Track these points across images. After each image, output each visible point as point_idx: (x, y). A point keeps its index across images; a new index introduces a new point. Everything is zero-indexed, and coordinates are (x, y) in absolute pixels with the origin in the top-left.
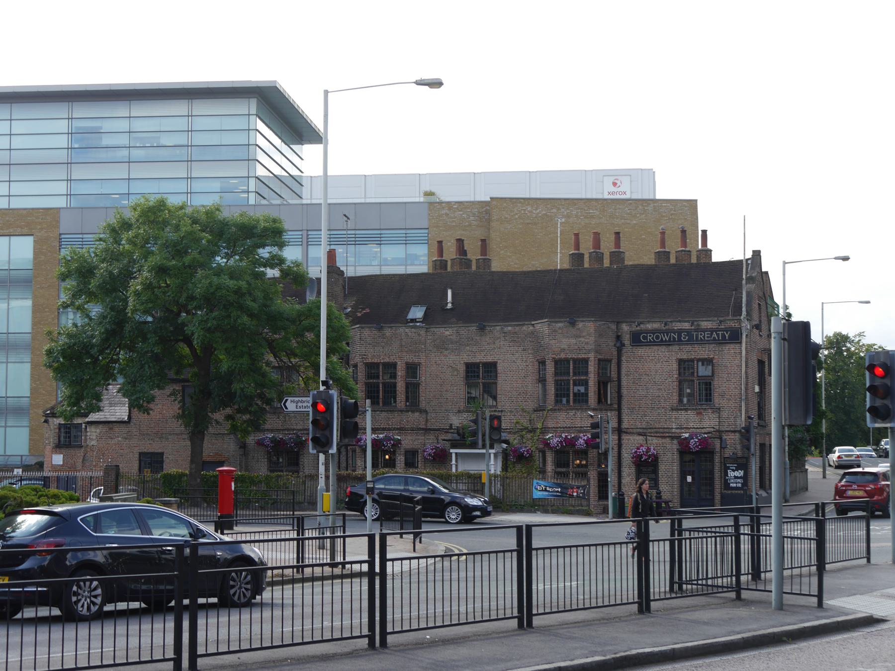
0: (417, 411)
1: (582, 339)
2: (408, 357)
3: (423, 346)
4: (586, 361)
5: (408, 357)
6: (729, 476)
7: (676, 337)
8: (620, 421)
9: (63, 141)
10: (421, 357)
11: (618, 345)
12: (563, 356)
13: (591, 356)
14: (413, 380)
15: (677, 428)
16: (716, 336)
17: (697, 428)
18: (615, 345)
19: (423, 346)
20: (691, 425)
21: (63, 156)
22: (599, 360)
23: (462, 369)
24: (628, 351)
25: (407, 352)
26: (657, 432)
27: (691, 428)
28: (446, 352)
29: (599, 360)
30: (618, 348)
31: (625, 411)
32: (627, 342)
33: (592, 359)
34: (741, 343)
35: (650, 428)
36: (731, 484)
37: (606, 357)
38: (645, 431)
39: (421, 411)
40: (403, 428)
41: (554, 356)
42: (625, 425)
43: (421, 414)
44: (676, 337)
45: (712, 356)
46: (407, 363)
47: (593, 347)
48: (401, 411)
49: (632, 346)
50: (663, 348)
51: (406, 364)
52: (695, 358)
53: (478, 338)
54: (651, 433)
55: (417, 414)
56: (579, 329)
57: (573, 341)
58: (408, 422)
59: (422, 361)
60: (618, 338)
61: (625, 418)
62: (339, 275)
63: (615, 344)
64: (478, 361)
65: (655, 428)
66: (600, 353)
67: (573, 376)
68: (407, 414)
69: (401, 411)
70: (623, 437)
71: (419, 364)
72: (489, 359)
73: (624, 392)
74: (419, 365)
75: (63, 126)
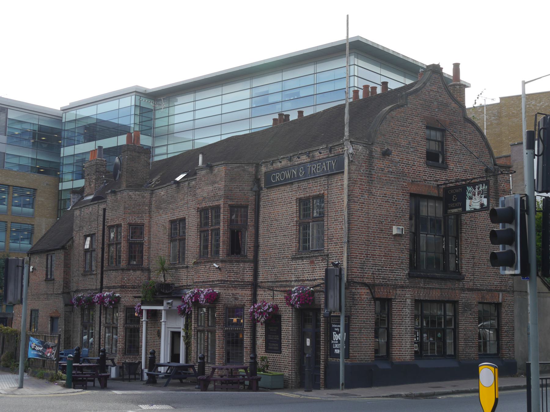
0: (138, 270)
1: (216, 185)
2: (131, 218)
3: (147, 208)
4: (218, 207)
5: (131, 218)
6: (334, 340)
7: (295, 173)
8: (256, 274)
9: (247, 104)
10: (144, 218)
11: (255, 188)
12: (204, 205)
13: (221, 202)
14: (138, 240)
15: (296, 281)
16: (325, 167)
17: (310, 280)
18: (251, 189)
19: (147, 208)
20: (306, 276)
21: (247, 114)
22: (231, 206)
23: (168, 225)
24: (264, 192)
25: (129, 213)
26: (281, 286)
27: (306, 280)
28: (161, 211)
29: (231, 206)
30: (255, 191)
31: (261, 263)
32: (263, 185)
33: (222, 206)
34: (343, 172)
35: (277, 281)
36: (336, 350)
37: (239, 203)
38: (274, 285)
39: (142, 270)
40: (123, 286)
41: (198, 206)
42: (260, 279)
43: (143, 272)
44: (295, 173)
45: (322, 192)
46: (130, 224)
47: (222, 193)
48: (123, 270)
49: (267, 188)
50: (288, 188)
51: (130, 226)
52: (310, 196)
53: (176, 195)
54: (277, 287)
55: (138, 273)
56: (214, 175)
57: (211, 188)
58: (129, 280)
59: (146, 222)
60: (257, 181)
61: (261, 270)
62: (139, 152)
63: (252, 189)
64: (176, 218)
65: (281, 281)
66: (231, 199)
67: (212, 226)
68: (129, 272)
69: (123, 270)
70: (258, 293)
71: (143, 225)
72: (181, 216)
73: (261, 241)
74: (143, 226)
75: (247, 94)
